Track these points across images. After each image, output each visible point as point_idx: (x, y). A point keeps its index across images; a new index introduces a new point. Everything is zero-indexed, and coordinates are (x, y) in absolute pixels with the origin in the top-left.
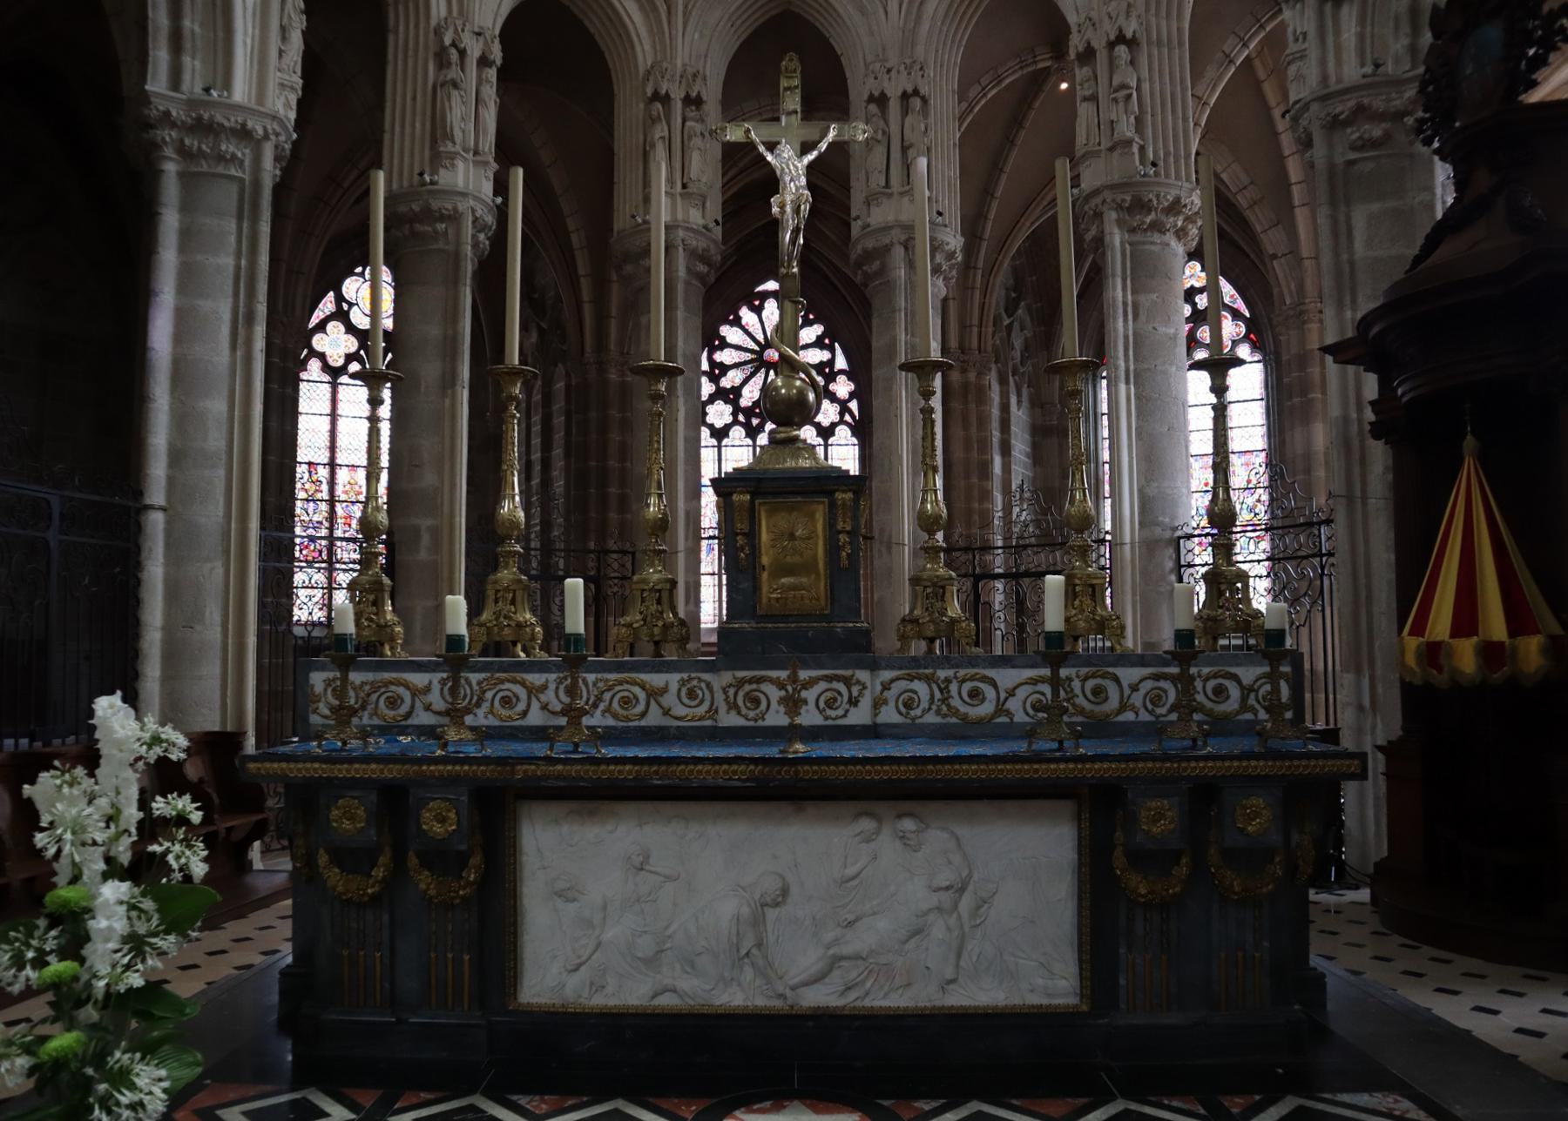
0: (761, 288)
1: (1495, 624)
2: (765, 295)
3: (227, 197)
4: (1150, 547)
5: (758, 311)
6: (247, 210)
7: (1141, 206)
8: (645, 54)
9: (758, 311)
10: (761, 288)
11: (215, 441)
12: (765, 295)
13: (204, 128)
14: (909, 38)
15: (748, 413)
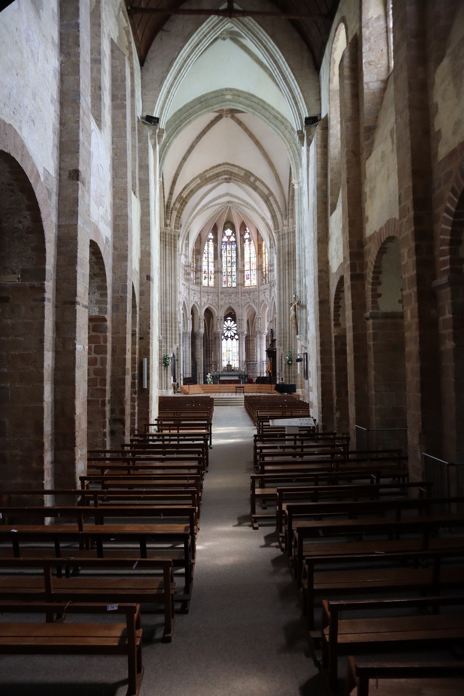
0: (227, 319)
1: (269, 370)
2: (228, 320)
3: (188, 338)
4: (261, 362)
5: (227, 322)
6: (189, 338)
7: (260, 333)
8: (217, 314)
9: (227, 322)
10: (227, 319)
11: (188, 356)
12: (228, 320)
13: (186, 333)
14: (242, 313)
15: (226, 337)
